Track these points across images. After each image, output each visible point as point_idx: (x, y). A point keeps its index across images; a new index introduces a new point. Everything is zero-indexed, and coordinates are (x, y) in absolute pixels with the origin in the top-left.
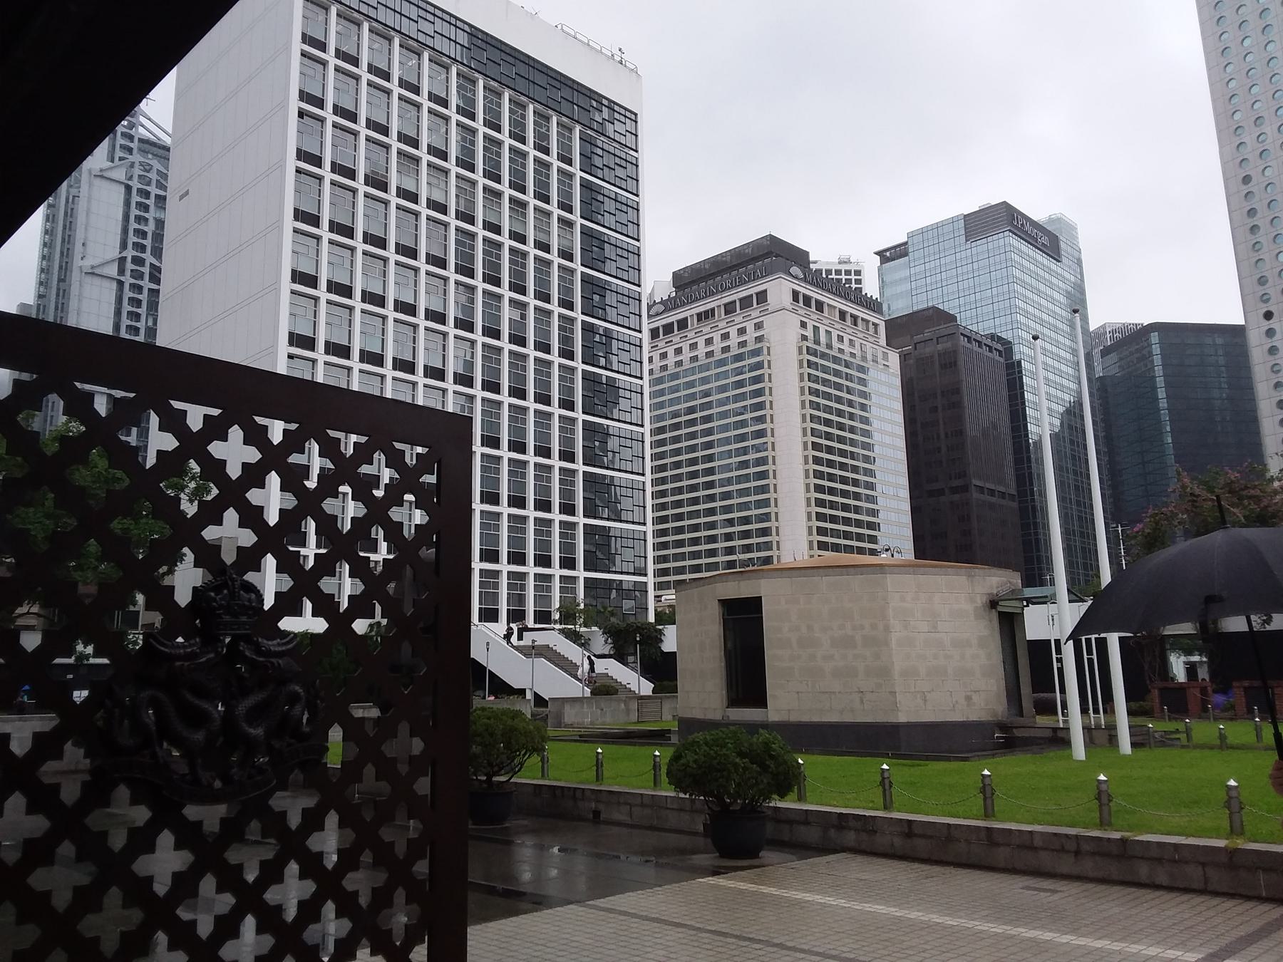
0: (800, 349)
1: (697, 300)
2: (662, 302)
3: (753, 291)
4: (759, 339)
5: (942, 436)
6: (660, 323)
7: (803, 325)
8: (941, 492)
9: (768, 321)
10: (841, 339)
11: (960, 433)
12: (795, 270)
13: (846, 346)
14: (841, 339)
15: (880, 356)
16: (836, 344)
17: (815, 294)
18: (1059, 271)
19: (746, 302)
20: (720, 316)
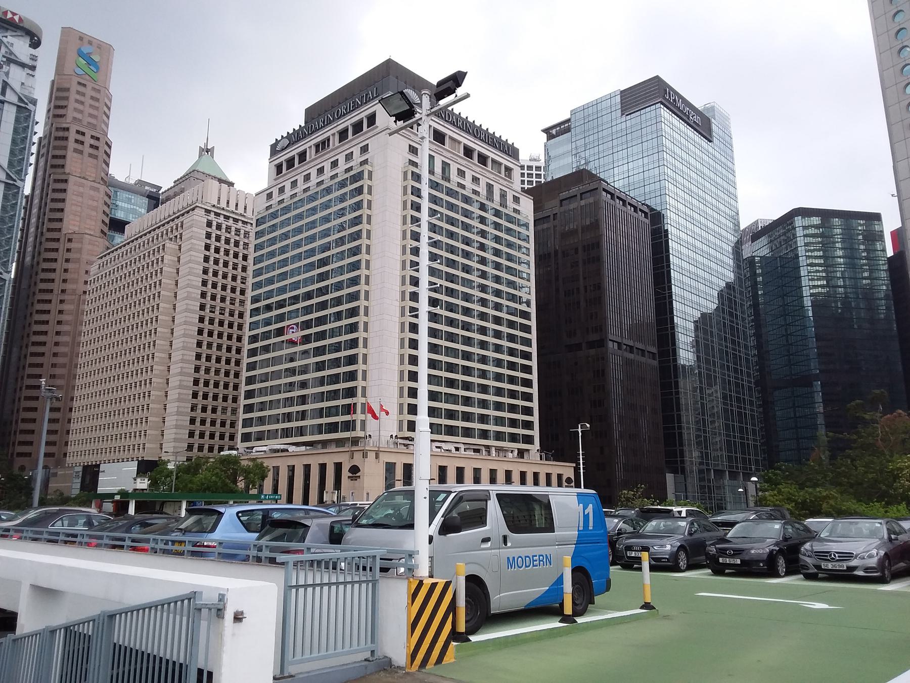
0: (405, 173)
1: (317, 130)
4: (365, 162)
5: (582, 289)
6: (283, 158)
7: (413, 150)
8: (578, 347)
9: (373, 144)
10: (461, 173)
11: (599, 287)
13: (468, 182)
14: (461, 173)
15: (510, 198)
18: (711, 150)
19: (358, 127)
20: (334, 145)
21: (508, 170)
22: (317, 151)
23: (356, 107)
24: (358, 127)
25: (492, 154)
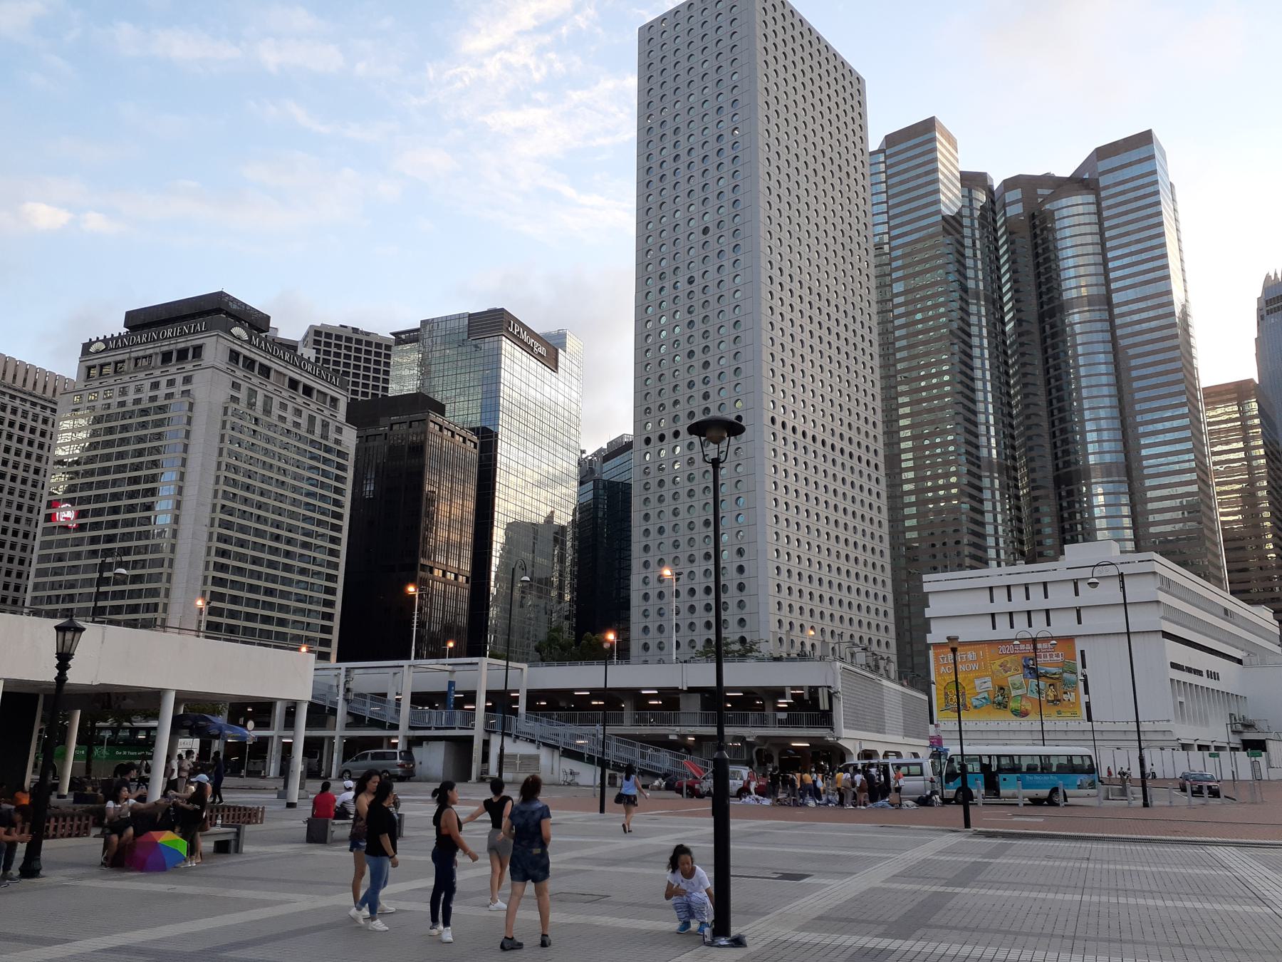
2: (105, 341)
3: (189, 344)
7: (235, 386)
9: (198, 377)
10: (283, 406)
12: (237, 331)
14: (283, 406)
15: (332, 428)
16: (276, 411)
17: (260, 358)
19: (182, 355)
21: (334, 401)
22: (136, 364)
23: (183, 334)
24: (182, 355)
25: (317, 385)
